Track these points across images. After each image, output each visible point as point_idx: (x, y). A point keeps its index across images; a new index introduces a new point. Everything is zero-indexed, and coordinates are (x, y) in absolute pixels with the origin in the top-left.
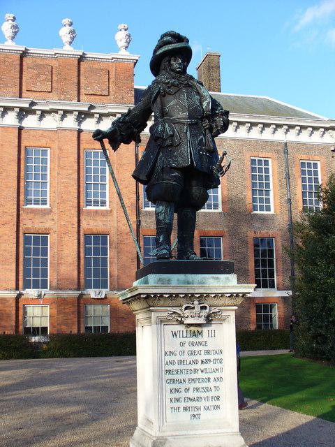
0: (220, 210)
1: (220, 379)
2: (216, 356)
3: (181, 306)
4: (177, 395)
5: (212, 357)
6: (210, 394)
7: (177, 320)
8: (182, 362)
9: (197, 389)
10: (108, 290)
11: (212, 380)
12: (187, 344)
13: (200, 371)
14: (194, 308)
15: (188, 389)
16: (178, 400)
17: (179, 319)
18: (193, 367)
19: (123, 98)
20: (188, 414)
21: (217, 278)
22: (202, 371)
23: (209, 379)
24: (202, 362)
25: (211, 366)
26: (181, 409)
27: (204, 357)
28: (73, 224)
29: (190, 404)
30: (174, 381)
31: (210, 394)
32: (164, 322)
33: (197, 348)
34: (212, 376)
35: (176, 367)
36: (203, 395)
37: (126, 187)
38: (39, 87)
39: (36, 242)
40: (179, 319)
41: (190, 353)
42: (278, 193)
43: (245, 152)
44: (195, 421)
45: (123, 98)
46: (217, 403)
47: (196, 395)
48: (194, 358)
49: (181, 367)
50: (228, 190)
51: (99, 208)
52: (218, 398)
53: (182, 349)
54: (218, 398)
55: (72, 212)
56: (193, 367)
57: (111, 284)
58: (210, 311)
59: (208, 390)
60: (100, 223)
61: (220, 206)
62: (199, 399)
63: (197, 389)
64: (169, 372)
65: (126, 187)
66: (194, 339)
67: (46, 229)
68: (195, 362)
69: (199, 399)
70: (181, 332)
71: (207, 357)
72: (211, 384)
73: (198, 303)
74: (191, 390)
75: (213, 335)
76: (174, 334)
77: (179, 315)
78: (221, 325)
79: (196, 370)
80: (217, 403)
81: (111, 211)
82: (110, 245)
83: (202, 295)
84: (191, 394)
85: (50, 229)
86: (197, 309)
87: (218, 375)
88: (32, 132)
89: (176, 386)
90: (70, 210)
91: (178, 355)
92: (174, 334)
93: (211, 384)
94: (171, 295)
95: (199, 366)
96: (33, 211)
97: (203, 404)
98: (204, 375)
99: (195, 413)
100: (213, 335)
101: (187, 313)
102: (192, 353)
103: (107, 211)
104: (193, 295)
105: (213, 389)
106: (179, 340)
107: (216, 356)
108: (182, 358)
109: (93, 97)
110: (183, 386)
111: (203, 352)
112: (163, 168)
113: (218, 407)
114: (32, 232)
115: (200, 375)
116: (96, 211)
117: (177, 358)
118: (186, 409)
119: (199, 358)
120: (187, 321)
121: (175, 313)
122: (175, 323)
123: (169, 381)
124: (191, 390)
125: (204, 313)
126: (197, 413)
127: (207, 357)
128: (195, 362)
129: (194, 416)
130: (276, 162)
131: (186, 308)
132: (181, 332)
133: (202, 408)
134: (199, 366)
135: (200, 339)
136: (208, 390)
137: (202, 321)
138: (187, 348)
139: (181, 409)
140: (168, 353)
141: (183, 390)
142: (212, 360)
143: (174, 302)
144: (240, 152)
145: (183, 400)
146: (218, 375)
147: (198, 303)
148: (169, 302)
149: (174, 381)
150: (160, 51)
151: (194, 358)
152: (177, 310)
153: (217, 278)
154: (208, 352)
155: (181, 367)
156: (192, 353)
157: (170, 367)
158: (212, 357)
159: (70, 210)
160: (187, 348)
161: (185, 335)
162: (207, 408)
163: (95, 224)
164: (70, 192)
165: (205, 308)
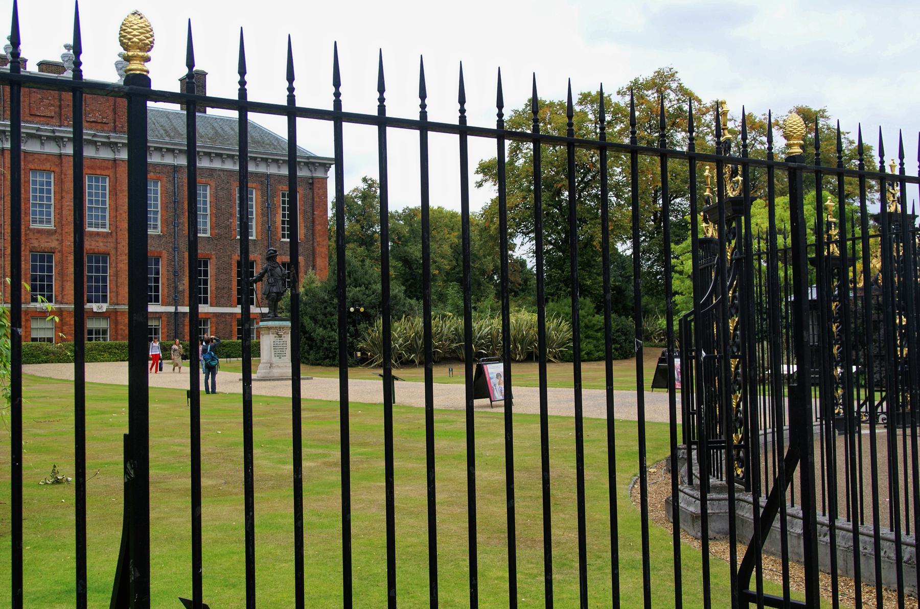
0: (208, 235)
38: (43, 111)
39: (42, 260)
42: (260, 221)
43: (232, 182)
51: (101, 230)
60: (101, 244)
61: (209, 231)
67: (51, 248)
81: (111, 233)
85: (55, 248)
88: (36, 156)
96: (39, 231)
103: (107, 233)
109: (93, 124)
114: (39, 250)
116: (98, 234)
130: (259, 193)
163: (97, 244)
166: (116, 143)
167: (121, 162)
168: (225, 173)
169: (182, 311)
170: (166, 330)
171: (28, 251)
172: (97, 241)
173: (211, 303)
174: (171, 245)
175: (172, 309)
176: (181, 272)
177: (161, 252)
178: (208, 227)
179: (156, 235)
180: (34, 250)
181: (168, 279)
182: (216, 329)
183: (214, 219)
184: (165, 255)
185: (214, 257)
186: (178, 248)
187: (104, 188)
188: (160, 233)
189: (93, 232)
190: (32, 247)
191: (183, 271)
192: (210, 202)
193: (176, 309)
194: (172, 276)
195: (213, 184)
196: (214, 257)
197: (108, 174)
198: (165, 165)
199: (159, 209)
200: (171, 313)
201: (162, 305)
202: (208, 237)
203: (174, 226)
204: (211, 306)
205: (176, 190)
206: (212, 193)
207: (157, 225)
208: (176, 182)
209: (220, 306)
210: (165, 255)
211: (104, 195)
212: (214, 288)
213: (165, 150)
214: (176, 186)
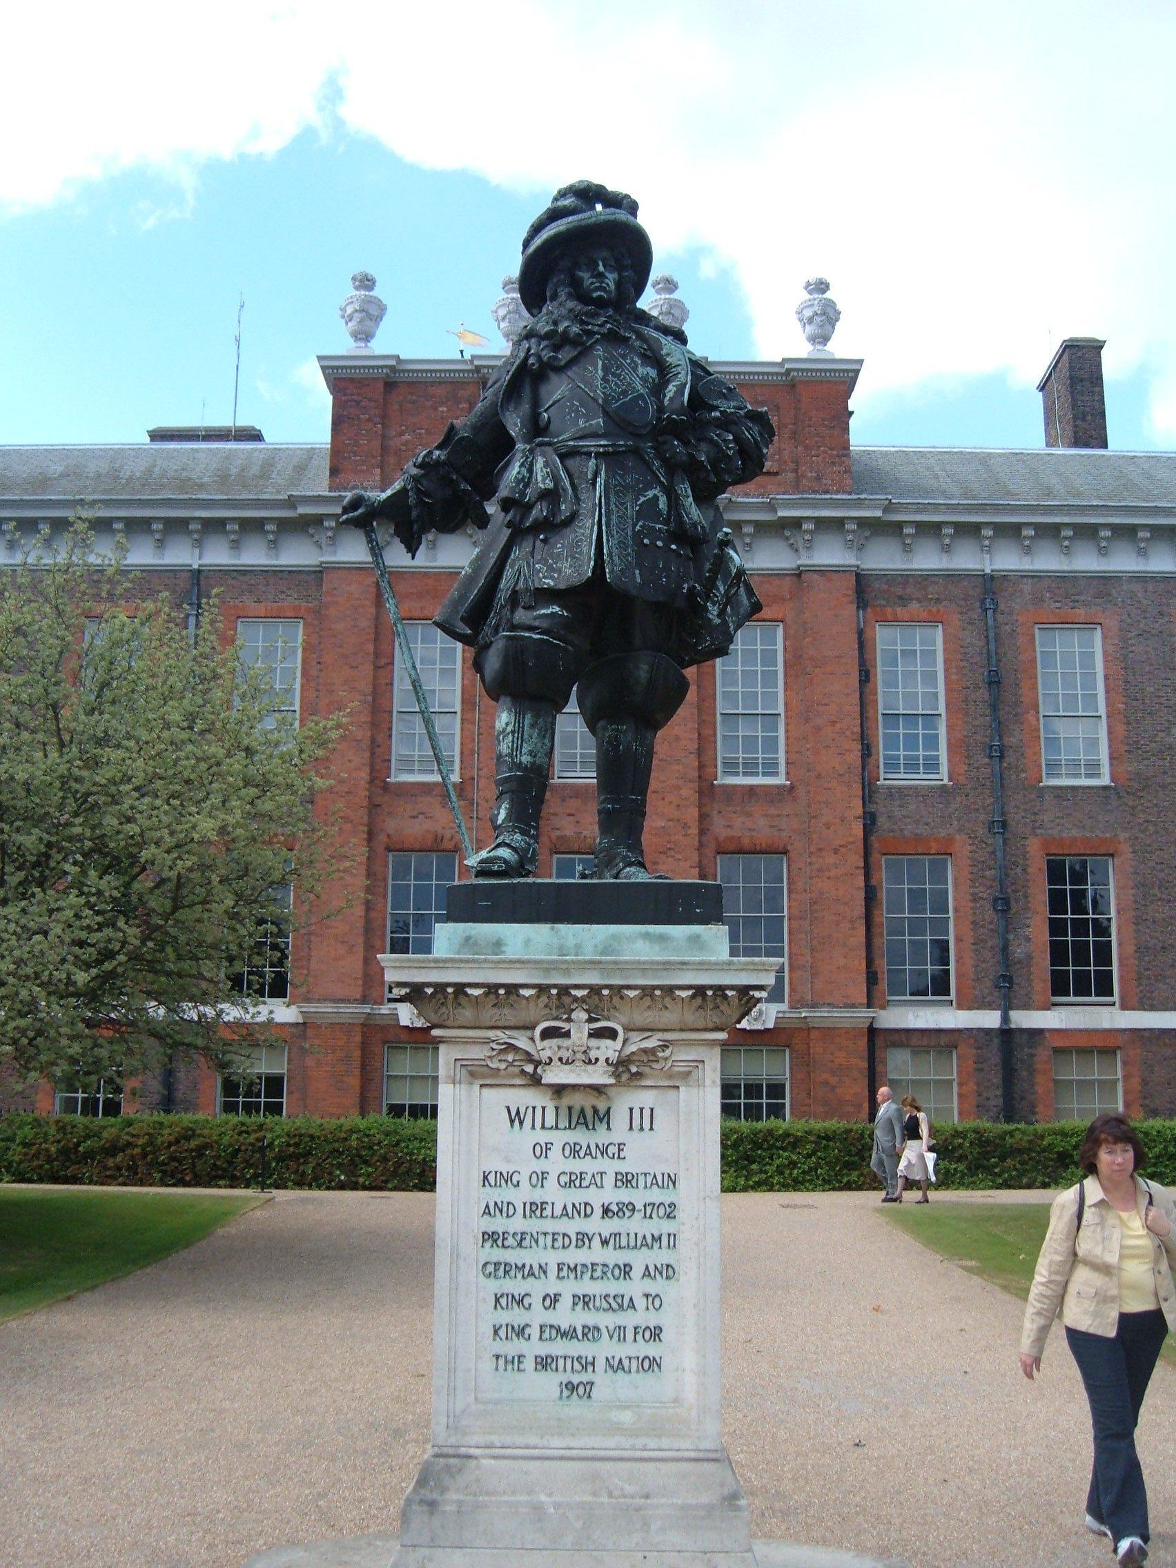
1: (668, 1272)
2: (656, 1195)
3: (533, 1028)
4: (516, 1316)
5: (638, 1197)
6: (629, 1320)
7: (523, 1072)
8: (536, 1209)
9: (584, 1301)
10: (784, 1007)
11: (637, 1272)
12: (555, 1152)
13: (596, 1242)
14: (567, 1034)
15: (555, 1299)
16: (521, 1332)
17: (529, 1068)
18: (572, 1226)
19: (818, 478)
20: (550, 1382)
21: (662, 938)
22: (605, 1242)
23: (626, 1270)
24: (606, 1211)
25: (635, 1225)
26: (529, 1364)
27: (611, 1195)
28: (686, 826)
29: (559, 1348)
30: (507, 1269)
31: (629, 1320)
32: (484, 1076)
33: (588, 1166)
34: (639, 1260)
35: (517, 1224)
36: (607, 1320)
37: (833, 723)
40: (529, 1068)
41: (564, 1179)
44: (576, 1408)
45: (818, 478)
46: (652, 1350)
47: (582, 1318)
48: (576, 1196)
49: (534, 1225)
50: (1128, 723)
52: (656, 1334)
53: (539, 1166)
54: (656, 1334)
55: (685, 792)
56: (572, 1226)
57: (792, 990)
58: (625, 1041)
59: (623, 1304)
60: (762, 822)
61: (1106, 770)
62: (590, 1333)
63: (584, 1301)
64: (490, 1237)
65: (833, 723)
66: (580, 1136)
68: (584, 1211)
69: (590, 1333)
70: (539, 1112)
71: (624, 1195)
72: (635, 1287)
73: (585, 1016)
74: (566, 1301)
75: (646, 1125)
76: (516, 1118)
77: (529, 1058)
78: (672, 1092)
79: (583, 1239)
80: (652, 1350)
81: (792, 788)
82: (789, 884)
83: (595, 990)
84: (564, 1316)
86: (579, 1029)
87: (660, 1256)
89: (515, 1286)
90: (678, 788)
91: (525, 1183)
92: (516, 1118)
93: (635, 1287)
94: (492, 989)
95: (596, 1225)
97: (604, 1349)
98: (611, 1256)
99: (576, 1379)
100: (646, 1125)
101: (547, 1049)
102: (573, 1181)
104: (564, 990)
105: (640, 1303)
106: (529, 1136)
107: (656, 1195)
108: (538, 1196)
110: (537, 1288)
111: (609, 1180)
112: (515, 592)
113: (651, 1364)
114: (576, 848)
115: (597, 1254)
117: (522, 1195)
118: (544, 1363)
119: (597, 1198)
120: (554, 1076)
121: (511, 1048)
122: (518, 1082)
123: (490, 1268)
124: (566, 1301)
125: (608, 1049)
126: (584, 1377)
127: (624, 1195)
128: (584, 1211)
129: (572, 1387)
131: (547, 1034)
132: (539, 1112)
133: (601, 1364)
134: (596, 1225)
135: (601, 1136)
136: (623, 1304)
137: (598, 1075)
138: (557, 1163)
139: (529, 1364)
140: (491, 1178)
141: (536, 1301)
142: (639, 1206)
143: (508, 1016)
144: (1161, 614)
145: (534, 1332)
146: (660, 1256)
147: (585, 1016)
148: (489, 1014)
149: (507, 1269)
150: (538, 242)
151: (576, 1196)
152: (522, 1042)
153: (662, 938)
154: (625, 1180)
155: (534, 1225)
156: (573, 1181)
157: (498, 1224)
158: (638, 1197)
159: (678, 788)
160: (557, 1163)
161: (550, 1120)
162: (616, 1366)
164: (678, 738)
165: (611, 1034)
166: (796, 523)
167: (815, 576)
168: (1150, 587)
169: (1025, 1026)
170: (972, 1086)
171: (547, 852)
172: (749, 815)
173: (1122, 998)
174: (982, 817)
175: (990, 1019)
176: (1017, 901)
177: (950, 840)
178: (1104, 756)
179: (932, 787)
180: (563, 849)
181: (973, 923)
182: (1145, 1082)
183: (1121, 729)
184: (962, 846)
185: (1125, 848)
186: (1004, 824)
187: (769, 658)
188: (946, 781)
189: (735, 787)
190: (558, 838)
191: (1026, 897)
192: (1106, 678)
193: (1005, 1019)
194: (990, 914)
195: (1112, 622)
196: (1125, 848)
197: (780, 616)
198: (952, 577)
199: (942, 709)
200: (988, 1032)
201: (960, 1007)
202: (1105, 788)
203: (991, 757)
204: (1124, 1007)
205: (992, 647)
206: (1110, 649)
207: (937, 758)
208: (990, 622)
209: (1152, 1008)
210: (962, 846)
211: (769, 678)
212: (1130, 949)
213: (951, 531)
214: (991, 634)
